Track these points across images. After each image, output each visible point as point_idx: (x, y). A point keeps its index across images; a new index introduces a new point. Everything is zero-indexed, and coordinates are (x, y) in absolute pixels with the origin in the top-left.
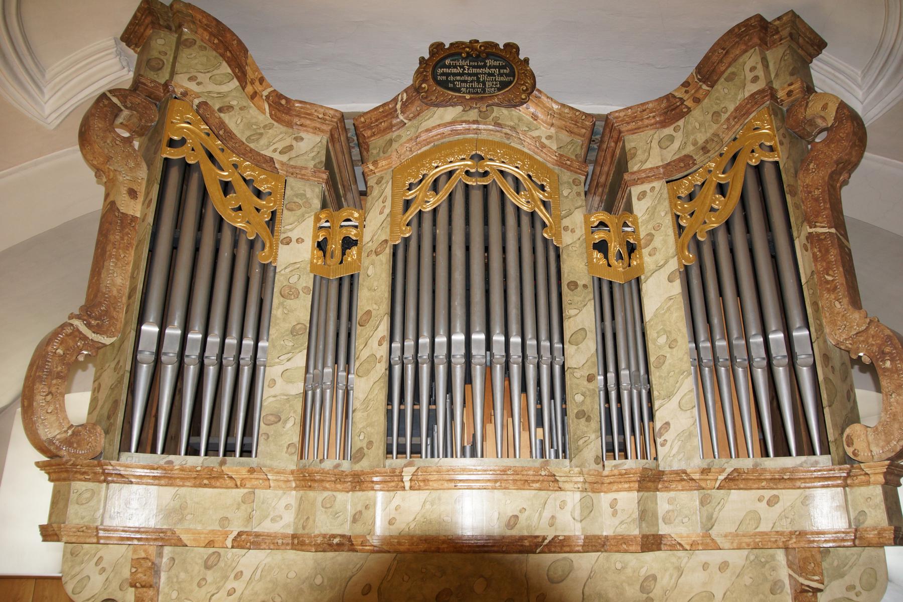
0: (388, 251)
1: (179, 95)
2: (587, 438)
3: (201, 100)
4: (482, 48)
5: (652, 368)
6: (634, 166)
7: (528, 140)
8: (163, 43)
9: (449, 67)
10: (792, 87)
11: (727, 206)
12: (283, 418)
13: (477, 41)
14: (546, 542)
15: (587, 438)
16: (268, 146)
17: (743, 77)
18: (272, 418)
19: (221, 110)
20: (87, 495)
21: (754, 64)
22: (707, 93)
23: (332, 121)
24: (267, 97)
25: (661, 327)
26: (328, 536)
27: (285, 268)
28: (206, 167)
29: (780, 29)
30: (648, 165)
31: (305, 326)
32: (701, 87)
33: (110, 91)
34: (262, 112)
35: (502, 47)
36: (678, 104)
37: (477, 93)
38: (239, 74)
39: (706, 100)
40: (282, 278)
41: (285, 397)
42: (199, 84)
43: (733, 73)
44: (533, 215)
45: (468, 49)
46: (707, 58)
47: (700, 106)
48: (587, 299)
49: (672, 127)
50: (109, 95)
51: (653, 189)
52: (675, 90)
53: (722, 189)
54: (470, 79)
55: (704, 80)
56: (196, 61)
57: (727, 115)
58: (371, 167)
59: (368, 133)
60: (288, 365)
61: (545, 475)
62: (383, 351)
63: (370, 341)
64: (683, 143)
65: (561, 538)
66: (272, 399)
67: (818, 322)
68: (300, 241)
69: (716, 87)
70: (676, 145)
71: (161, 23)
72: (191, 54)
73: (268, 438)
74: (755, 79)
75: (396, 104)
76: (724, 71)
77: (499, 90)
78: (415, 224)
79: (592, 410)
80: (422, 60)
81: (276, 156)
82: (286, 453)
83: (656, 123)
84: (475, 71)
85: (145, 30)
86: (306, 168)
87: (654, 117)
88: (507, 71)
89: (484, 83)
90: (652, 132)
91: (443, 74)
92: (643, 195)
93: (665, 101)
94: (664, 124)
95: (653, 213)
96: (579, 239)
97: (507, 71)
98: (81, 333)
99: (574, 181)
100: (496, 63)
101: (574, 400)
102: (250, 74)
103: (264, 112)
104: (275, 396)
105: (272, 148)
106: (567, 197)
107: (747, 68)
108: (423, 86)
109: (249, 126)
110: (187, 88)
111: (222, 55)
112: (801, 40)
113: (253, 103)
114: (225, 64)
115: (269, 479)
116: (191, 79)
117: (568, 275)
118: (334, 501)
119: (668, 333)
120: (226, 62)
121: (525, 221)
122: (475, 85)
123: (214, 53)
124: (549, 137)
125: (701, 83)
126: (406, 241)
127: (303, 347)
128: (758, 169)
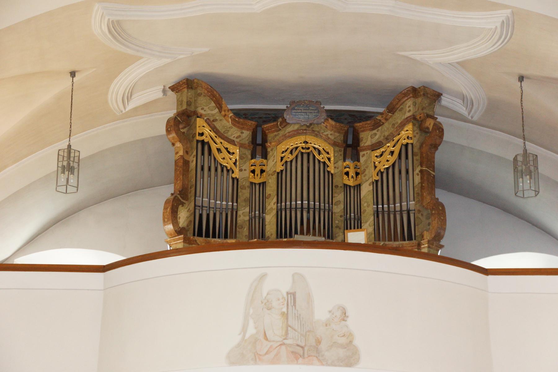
0: (276, 174)
1: (199, 116)
5: (362, 214)
6: (362, 144)
7: (323, 136)
9: (296, 110)
10: (421, 116)
11: (392, 159)
16: (232, 135)
17: (405, 110)
19: (213, 121)
21: (410, 105)
22: (391, 116)
25: (365, 200)
27: (242, 179)
30: (366, 144)
32: (388, 115)
34: (228, 122)
38: (219, 107)
39: (391, 119)
40: (240, 183)
42: (205, 111)
43: (402, 108)
44: (324, 163)
45: (303, 103)
47: (388, 121)
49: (376, 130)
51: (367, 153)
53: (392, 153)
54: (303, 114)
55: (389, 112)
56: (203, 102)
57: (397, 125)
58: (269, 144)
59: (267, 132)
60: (244, 211)
62: (275, 207)
63: (270, 204)
66: (239, 221)
67: (418, 199)
68: (245, 170)
69: (395, 114)
70: (377, 137)
72: (201, 99)
73: (239, 233)
75: (278, 123)
76: (398, 108)
78: (285, 164)
81: (234, 139)
83: (370, 129)
84: (305, 111)
85: (182, 89)
86: (246, 144)
90: (369, 132)
91: (294, 112)
94: (373, 129)
95: (366, 162)
99: (339, 151)
103: (229, 122)
104: (241, 220)
105: (233, 136)
106: (336, 156)
107: (407, 106)
108: (287, 116)
109: (224, 127)
110: (202, 113)
111: (212, 99)
112: (429, 95)
114: (213, 102)
116: (202, 109)
119: (367, 202)
120: (213, 101)
121: (322, 165)
123: (208, 98)
124: (331, 134)
126: (282, 171)
128: (407, 145)
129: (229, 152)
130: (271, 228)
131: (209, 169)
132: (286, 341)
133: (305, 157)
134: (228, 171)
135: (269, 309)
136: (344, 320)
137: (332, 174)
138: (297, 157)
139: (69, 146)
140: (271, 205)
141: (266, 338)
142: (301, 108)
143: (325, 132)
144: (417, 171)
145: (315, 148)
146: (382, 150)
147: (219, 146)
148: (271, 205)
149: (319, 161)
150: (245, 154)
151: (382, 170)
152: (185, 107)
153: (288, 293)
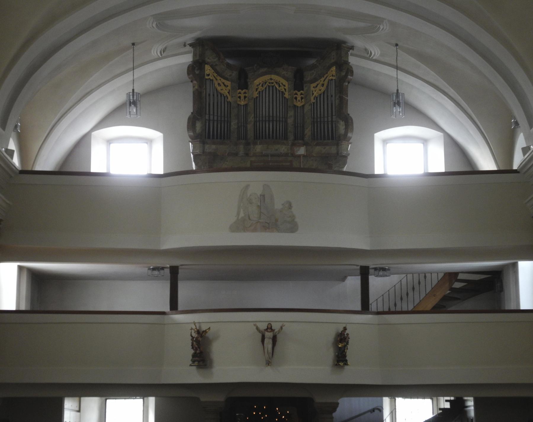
11: (323, 89)
24: (226, 63)
42: (210, 59)
62: (253, 120)
70: (314, 74)
116: (208, 58)
121: (281, 93)
126: (257, 97)
129: (225, 85)
130: (251, 134)
131: (214, 95)
132: (260, 220)
133: (271, 88)
134: (224, 97)
135: (251, 203)
136: (290, 209)
137: (287, 99)
138: (266, 88)
139: (133, 90)
140: (251, 118)
141: (250, 219)
144: (337, 97)
146: (317, 83)
147: (220, 82)
148: (251, 118)
149: (279, 91)
151: (317, 96)
152: (198, 58)
153: (261, 195)
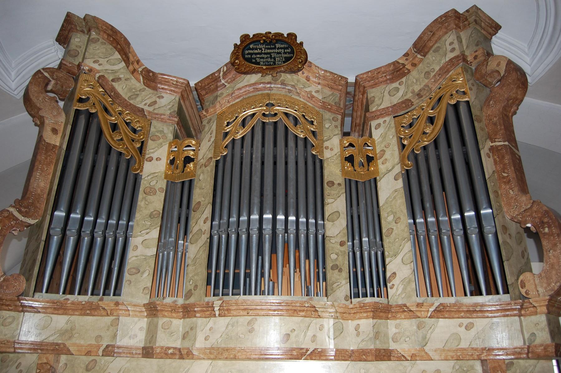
0: (213, 164)
1: (87, 72)
2: (340, 283)
3: (100, 74)
4: (273, 37)
5: (384, 237)
6: (373, 108)
7: (303, 93)
8: (79, 41)
9: (253, 49)
10: (477, 53)
12: (141, 270)
13: (270, 33)
14: (309, 352)
15: (340, 283)
16: (142, 102)
17: (444, 49)
18: (134, 271)
19: (113, 80)
20: (10, 320)
21: (452, 41)
22: (421, 61)
23: (182, 86)
25: (389, 209)
26: (165, 348)
27: (148, 176)
28: (101, 115)
29: (468, 18)
30: (382, 107)
31: (159, 212)
32: (416, 56)
33: (43, 69)
34: (139, 82)
35: (286, 36)
36: (401, 67)
37: (270, 65)
38: (125, 59)
39: (421, 65)
40: (145, 182)
41: (144, 257)
43: (438, 47)
44: (306, 139)
45: (264, 38)
46: (420, 38)
47: (416, 69)
48: (341, 193)
49: (398, 82)
50: (42, 71)
51: (385, 121)
52: (399, 59)
53: (431, 120)
54: (265, 56)
55: (419, 51)
56: (99, 51)
57: (434, 73)
58: (204, 113)
59: (203, 93)
60: (147, 237)
61: (308, 307)
63: (199, 221)
64: (405, 92)
65: (319, 350)
66: (134, 258)
67: (498, 204)
68: (158, 159)
69: (427, 56)
71: (78, 28)
72: (96, 47)
73: (130, 283)
74: (453, 50)
75: (220, 73)
76: (432, 47)
77: (284, 62)
78: (230, 147)
79: (343, 265)
80: (236, 45)
81: (146, 108)
82: (142, 293)
83: (387, 80)
84: (269, 51)
86: (164, 115)
87: (385, 76)
88: (289, 50)
89: (274, 58)
90: (384, 86)
91: (249, 54)
92: (379, 126)
93: (392, 66)
94: (392, 80)
95: (385, 137)
96: (336, 155)
97: (289, 50)
98: (14, 216)
99: (333, 119)
100: (282, 46)
101: (330, 257)
102: (131, 58)
103: (140, 82)
105: (144, 103)
106: (328, 128)
107: (447, 43)
108: (236, 61)
109: (130, 90)
110: (92, 67)
111: (115, 48)
112: (483, 24)
113: (134, 77)
114: (117, 53)
115: (129, 310)
116: (95, 62)
117: (328, 177)
118: (171, 325)
119: (394, 213)
121: (301, 144)
122: (269, 60)
123: (111, 47)
124: (317, 92)
125: (416, 54)
126: (225, 157)
127: (157, 226)
128: (456, 107)
142: (260, 46)
143: (305, 87)
145: (286, 114)
150: (162, 132)
